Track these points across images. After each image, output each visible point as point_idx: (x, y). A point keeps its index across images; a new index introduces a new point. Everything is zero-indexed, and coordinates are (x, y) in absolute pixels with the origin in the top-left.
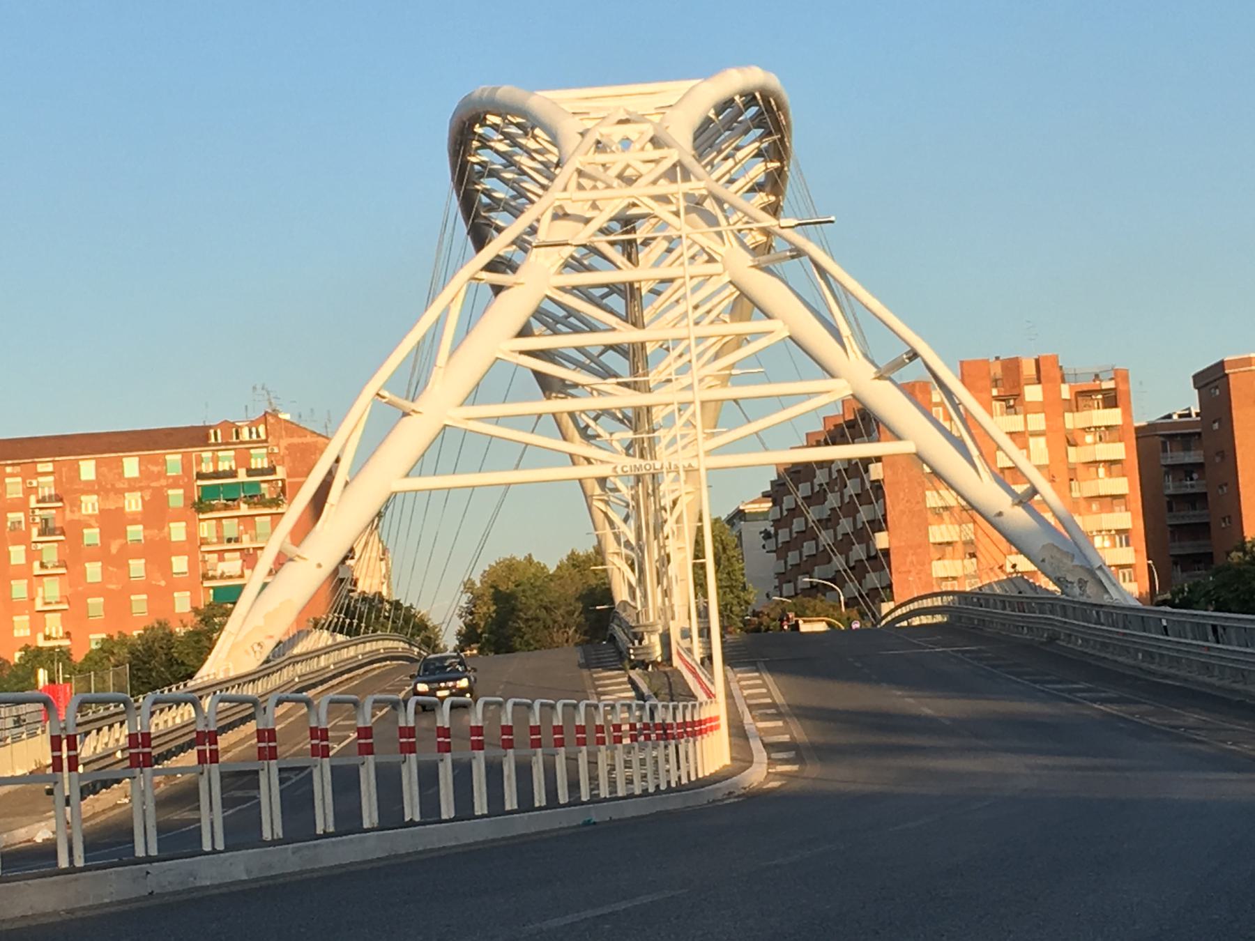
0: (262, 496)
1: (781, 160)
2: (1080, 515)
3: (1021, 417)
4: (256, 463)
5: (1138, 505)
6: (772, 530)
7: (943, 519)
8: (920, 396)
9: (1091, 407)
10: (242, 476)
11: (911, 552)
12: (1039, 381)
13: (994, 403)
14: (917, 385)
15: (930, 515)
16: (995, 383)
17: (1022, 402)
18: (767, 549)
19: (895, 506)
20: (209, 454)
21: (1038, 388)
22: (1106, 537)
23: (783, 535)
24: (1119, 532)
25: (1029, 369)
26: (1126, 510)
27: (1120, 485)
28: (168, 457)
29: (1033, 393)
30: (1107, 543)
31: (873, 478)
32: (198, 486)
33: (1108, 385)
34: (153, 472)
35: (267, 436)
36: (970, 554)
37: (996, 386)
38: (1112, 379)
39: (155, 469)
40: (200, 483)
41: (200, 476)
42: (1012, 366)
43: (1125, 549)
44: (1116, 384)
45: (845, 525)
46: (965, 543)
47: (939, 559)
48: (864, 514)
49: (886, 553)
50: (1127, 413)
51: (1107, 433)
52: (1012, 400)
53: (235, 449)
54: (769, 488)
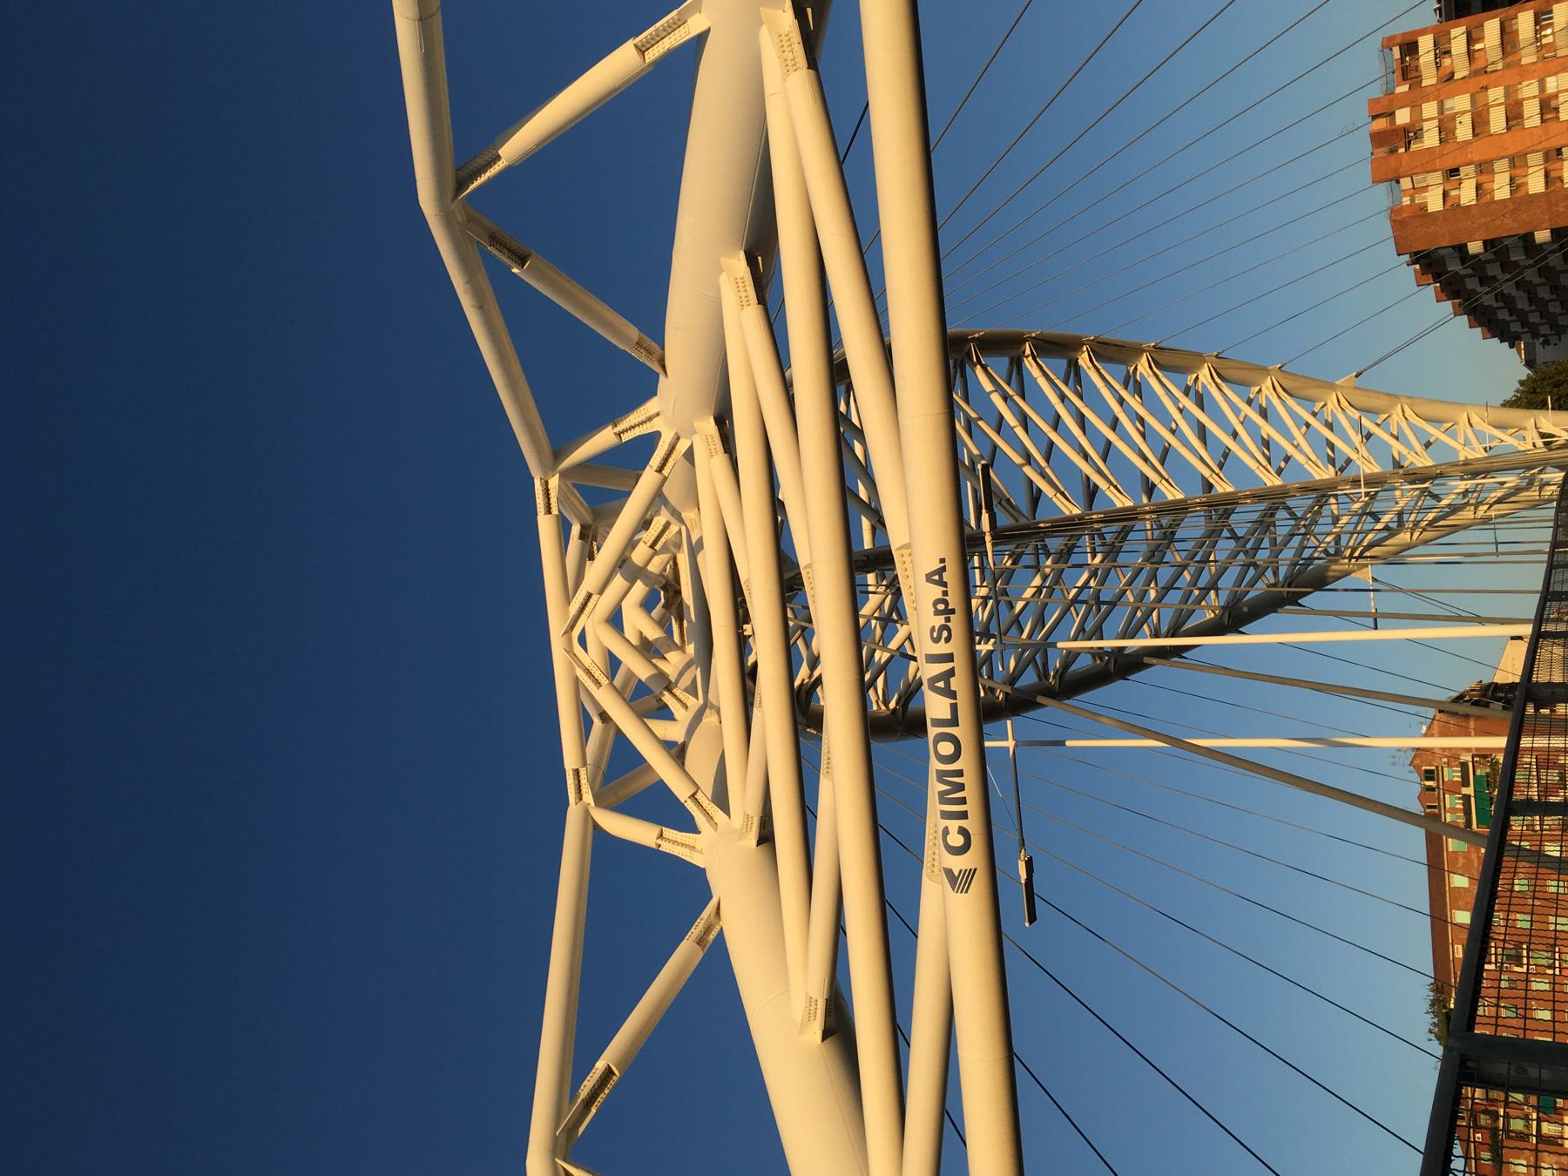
0: (1488, 775)
1: (1026, 340)
2: (1520, 60)
3: (1426, 125)
4: (1458, 776)
5: (1511, 10)
6: (1541, 339)
7: (1523, 183)
8: (1404, 215)
9: (1417, 68)
10: (1470, 791)
11: (1555, 209)
12: (1394, 113)
13: (1411, 150)
14: (1394, 218)
15: (1519, 195)
16: (1393, 151)
17: (1412, 124)
18: (1557, 342)
19: (1509, 227)
20: (1448, 815)
21: (1397, 112)
22: (1543, 33)
23: (1544, 330)
24: (1537, 22)
25: (1381, 124)
26: (1516, 18)
27: (1492, 27)
28: (1450, 850)
29: (1403, 117)
30: (1549, 31)
31: (1482, 250)
32: (1478, 827)
33: (1396, 52)
34: (1464, 863)
35: (1433, 765)
36: (1558, 155)
37: (1397, 150)
38: (1391, 50)
39: (1461, 861)
40: (1474, 826)
41: (1469, 823)
42: (1378, 139)
43: (1555, 14)
44: (1395, 46)
45: (1531, 275)
46: (1547, 159)
47: (1562, 181)
48: (1517, 256)
49: (1553, 231)
50: (1423, 32)
51: (1442, 51)
52: (1410, 134)
53: (1444, 795)
54: (1507, 343)
